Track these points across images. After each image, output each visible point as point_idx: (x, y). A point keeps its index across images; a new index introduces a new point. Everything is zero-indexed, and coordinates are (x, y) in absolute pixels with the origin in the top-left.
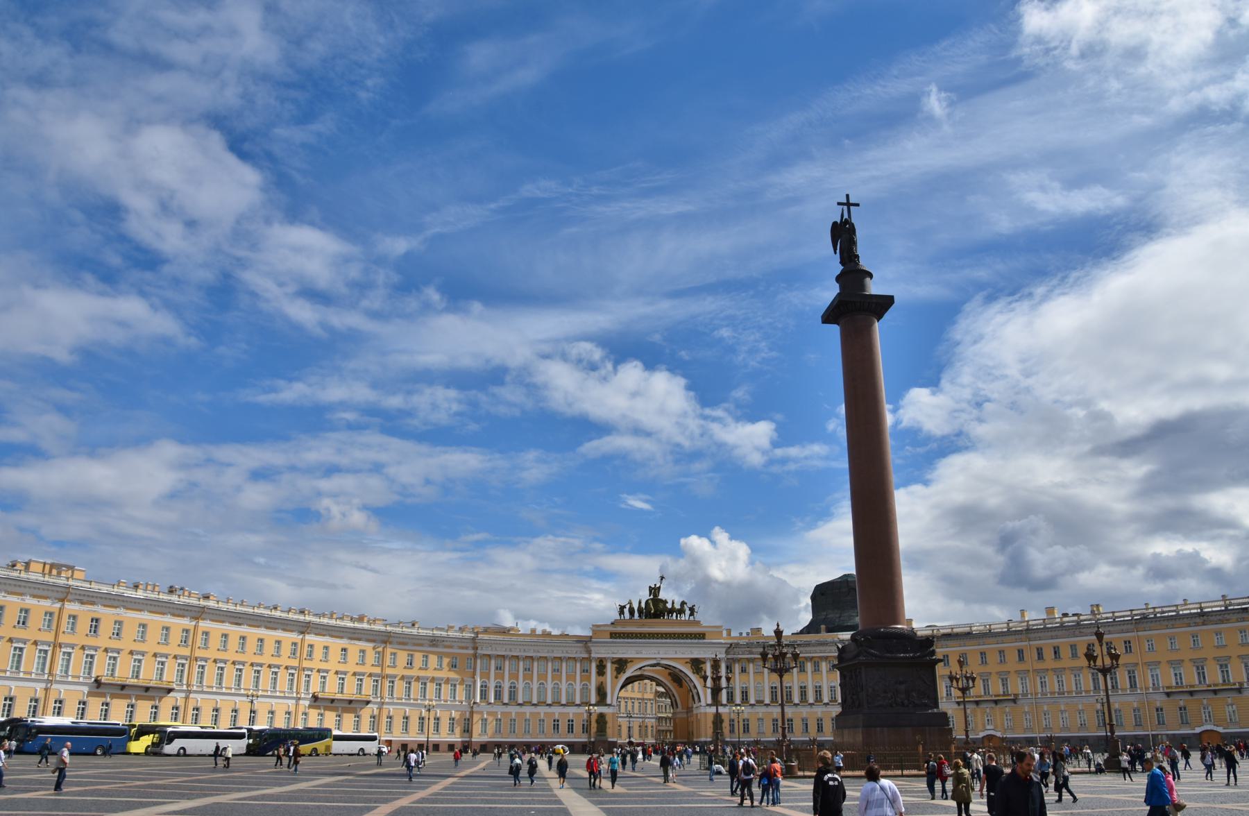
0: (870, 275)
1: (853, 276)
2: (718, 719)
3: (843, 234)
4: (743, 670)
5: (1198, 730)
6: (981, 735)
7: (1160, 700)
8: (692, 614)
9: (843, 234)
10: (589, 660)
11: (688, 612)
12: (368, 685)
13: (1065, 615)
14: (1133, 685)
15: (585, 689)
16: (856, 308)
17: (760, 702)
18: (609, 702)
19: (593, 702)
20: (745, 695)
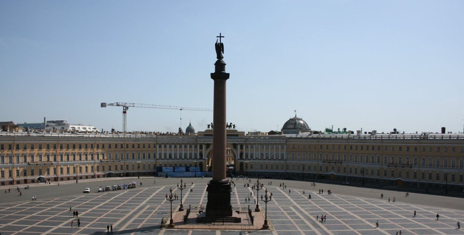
0: (226, 64)
1: (220, 65)
3: (219, 48)
4: (252, 147)
5: (396, 179)
6: (330, 173)
7: (385, 167)
9: (219, 48)
11: (233, 127)
13: (366, 133)
14: (378, 162)
16: (220, 76)
17: (257, 158)
18: (204, 158)
19: (198, 158)
20: (252, 156)
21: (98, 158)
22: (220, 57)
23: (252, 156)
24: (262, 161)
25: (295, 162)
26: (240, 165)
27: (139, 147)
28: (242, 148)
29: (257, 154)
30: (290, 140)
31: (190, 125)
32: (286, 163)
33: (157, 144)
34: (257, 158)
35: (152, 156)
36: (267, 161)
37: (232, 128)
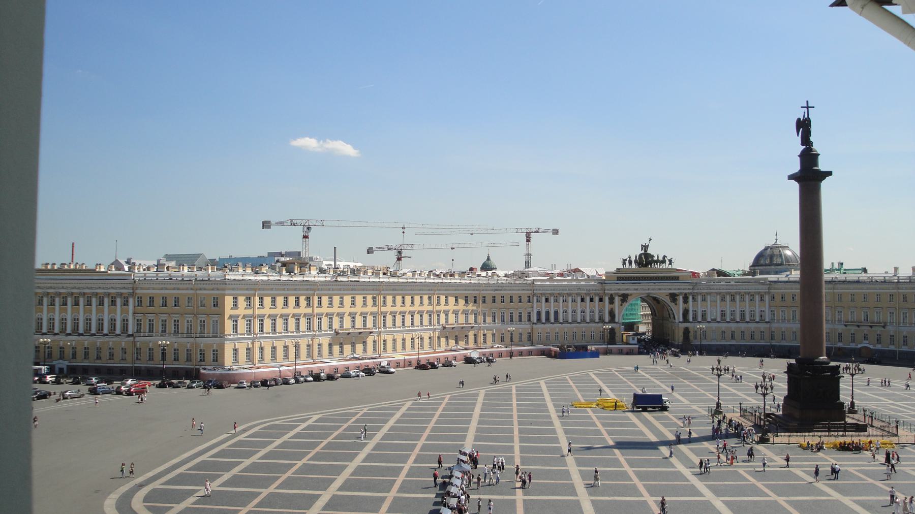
1: (809, 157)
2: (687, 331)
3: (804, 126)
4: (704, 300)
6: (859, 346)
8: (670, 264)
9: (804, 126)
10: (605, 294)
11: (667, 262)
12: (471, 319)
15: (601, 311)
16: (810, 176)
17: (714, 320)
19: (607, 320)
21: (439, 322)
22: (806, 140)
23: (704, 315)
24: (723, 326)
25: (788, 325)
26: (684, 333)
27: (503, 302)
28: (686, 300)
29: (714, 312)
30: (776, 286)
31: (488, 259)
32: (770, 328)
33: (534, 295)
34: (714, 320)
35: (525, 317)
36: (733, 326)
37: (666, 266)
